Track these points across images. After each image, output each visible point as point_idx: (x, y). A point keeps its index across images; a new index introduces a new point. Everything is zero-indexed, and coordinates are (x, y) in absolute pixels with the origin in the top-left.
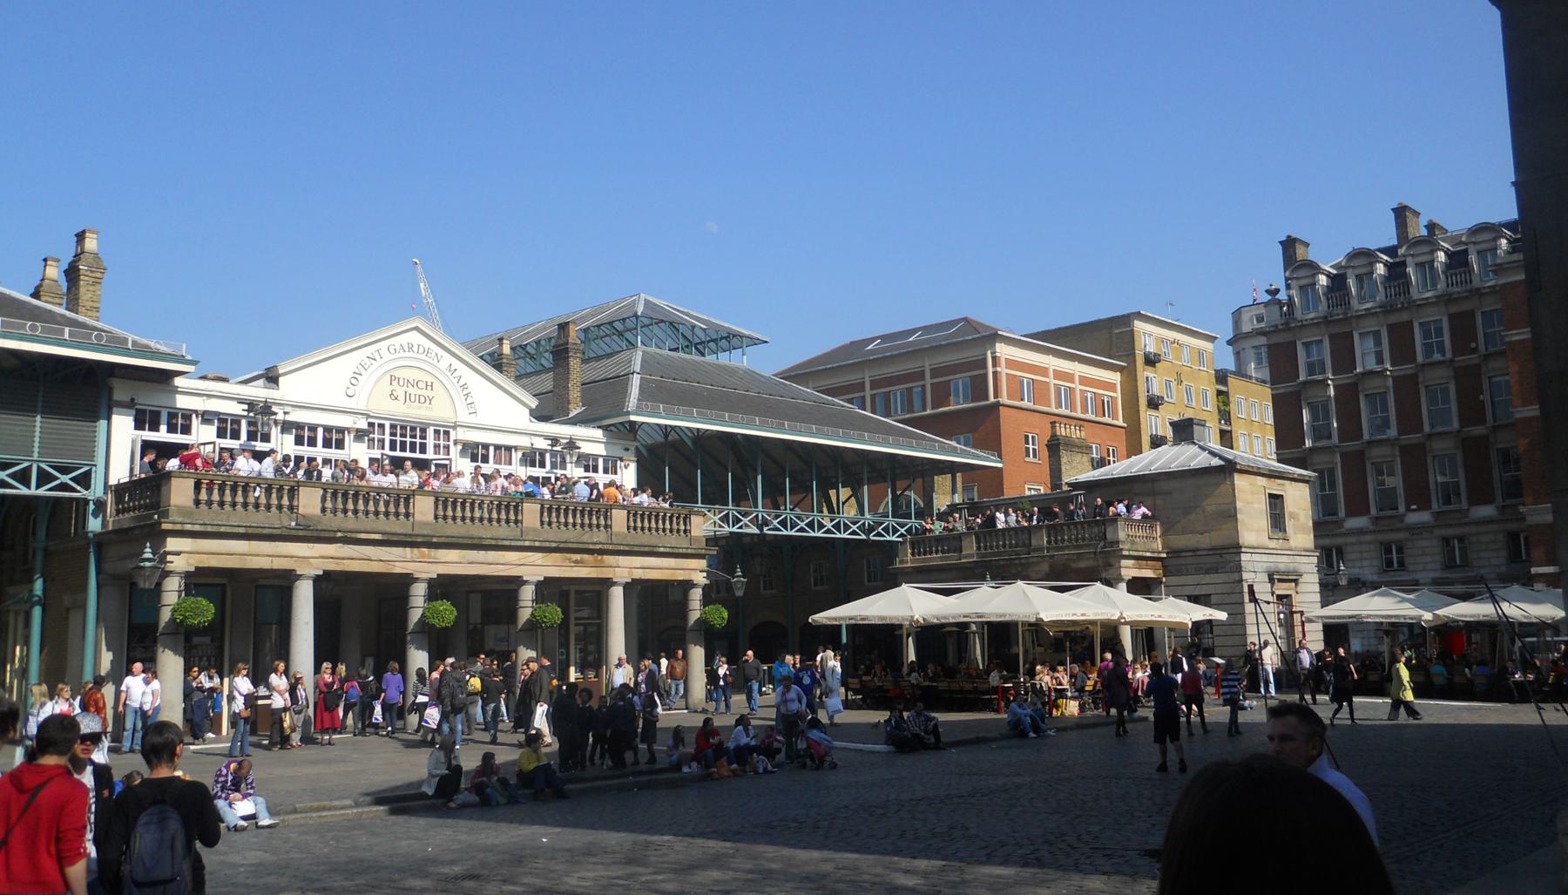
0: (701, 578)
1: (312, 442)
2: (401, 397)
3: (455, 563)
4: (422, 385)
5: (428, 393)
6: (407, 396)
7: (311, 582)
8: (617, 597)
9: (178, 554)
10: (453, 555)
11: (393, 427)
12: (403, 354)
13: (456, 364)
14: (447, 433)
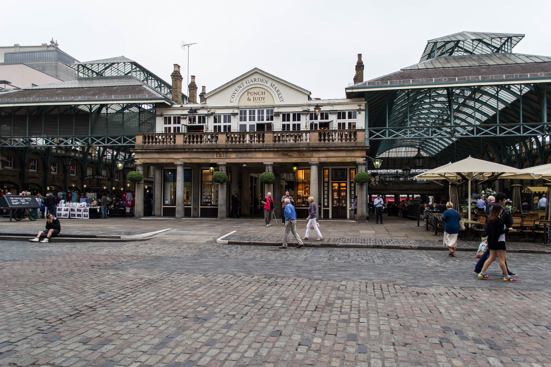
0: (361, 160)
1: (344, 118)
2: (252, 99)
3: (233, 158)
4: (260, 93)
5: (263, 96)
6: (254, 99)
9: (137, 159)
10: (233, 156)
12: (252, 83)
13: (274, 83)
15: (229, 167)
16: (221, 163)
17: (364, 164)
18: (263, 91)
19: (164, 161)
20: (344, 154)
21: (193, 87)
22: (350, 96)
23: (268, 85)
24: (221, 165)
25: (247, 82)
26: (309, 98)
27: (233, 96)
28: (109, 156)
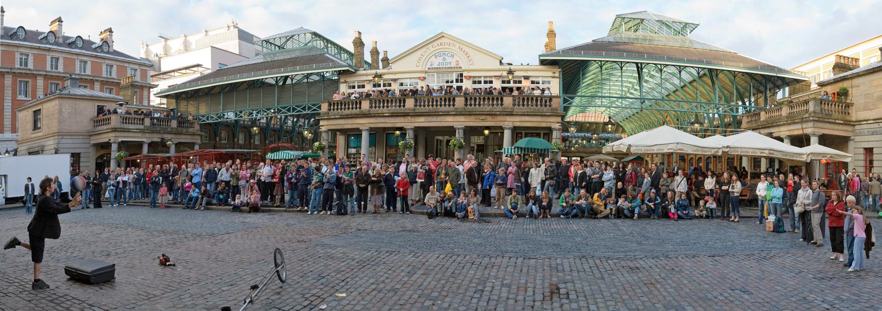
3: (422, 122)
14: (461, 75)
15: (417, 130)
17: (559, 130)
19: (349, 127)
20: (539, 119)
21: (375, 52)
22: (543, 62)
23: (456, 48)
26: (501, 63)
28: (290, 123)
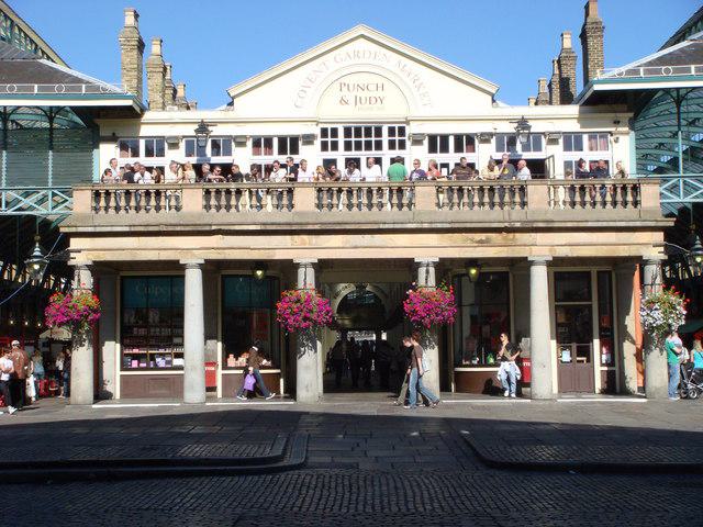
2: (352, 101)
4: (372, 87)
5: (380, 94)
6: (357, 100)
7: (545, 268)
8: (540, 282)
11: (347, 132)
14: (402, 131)
16: (303, 261)
18: (380, 81)
24: (306, 266)
25: (338, 59)
27: (302, 94)
